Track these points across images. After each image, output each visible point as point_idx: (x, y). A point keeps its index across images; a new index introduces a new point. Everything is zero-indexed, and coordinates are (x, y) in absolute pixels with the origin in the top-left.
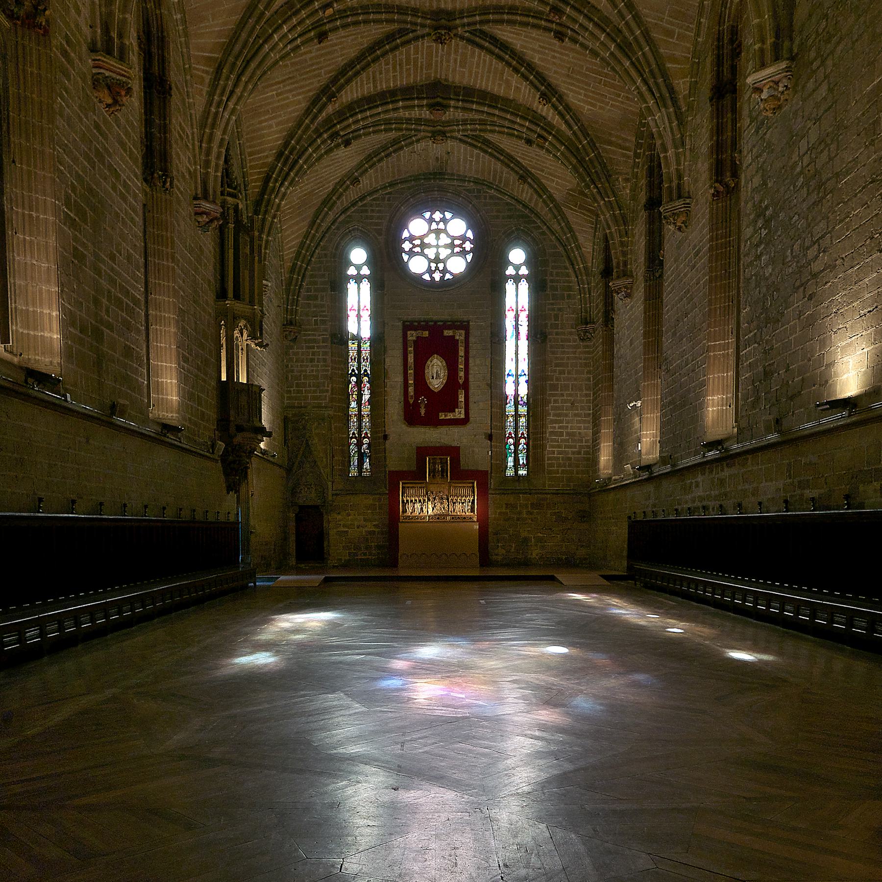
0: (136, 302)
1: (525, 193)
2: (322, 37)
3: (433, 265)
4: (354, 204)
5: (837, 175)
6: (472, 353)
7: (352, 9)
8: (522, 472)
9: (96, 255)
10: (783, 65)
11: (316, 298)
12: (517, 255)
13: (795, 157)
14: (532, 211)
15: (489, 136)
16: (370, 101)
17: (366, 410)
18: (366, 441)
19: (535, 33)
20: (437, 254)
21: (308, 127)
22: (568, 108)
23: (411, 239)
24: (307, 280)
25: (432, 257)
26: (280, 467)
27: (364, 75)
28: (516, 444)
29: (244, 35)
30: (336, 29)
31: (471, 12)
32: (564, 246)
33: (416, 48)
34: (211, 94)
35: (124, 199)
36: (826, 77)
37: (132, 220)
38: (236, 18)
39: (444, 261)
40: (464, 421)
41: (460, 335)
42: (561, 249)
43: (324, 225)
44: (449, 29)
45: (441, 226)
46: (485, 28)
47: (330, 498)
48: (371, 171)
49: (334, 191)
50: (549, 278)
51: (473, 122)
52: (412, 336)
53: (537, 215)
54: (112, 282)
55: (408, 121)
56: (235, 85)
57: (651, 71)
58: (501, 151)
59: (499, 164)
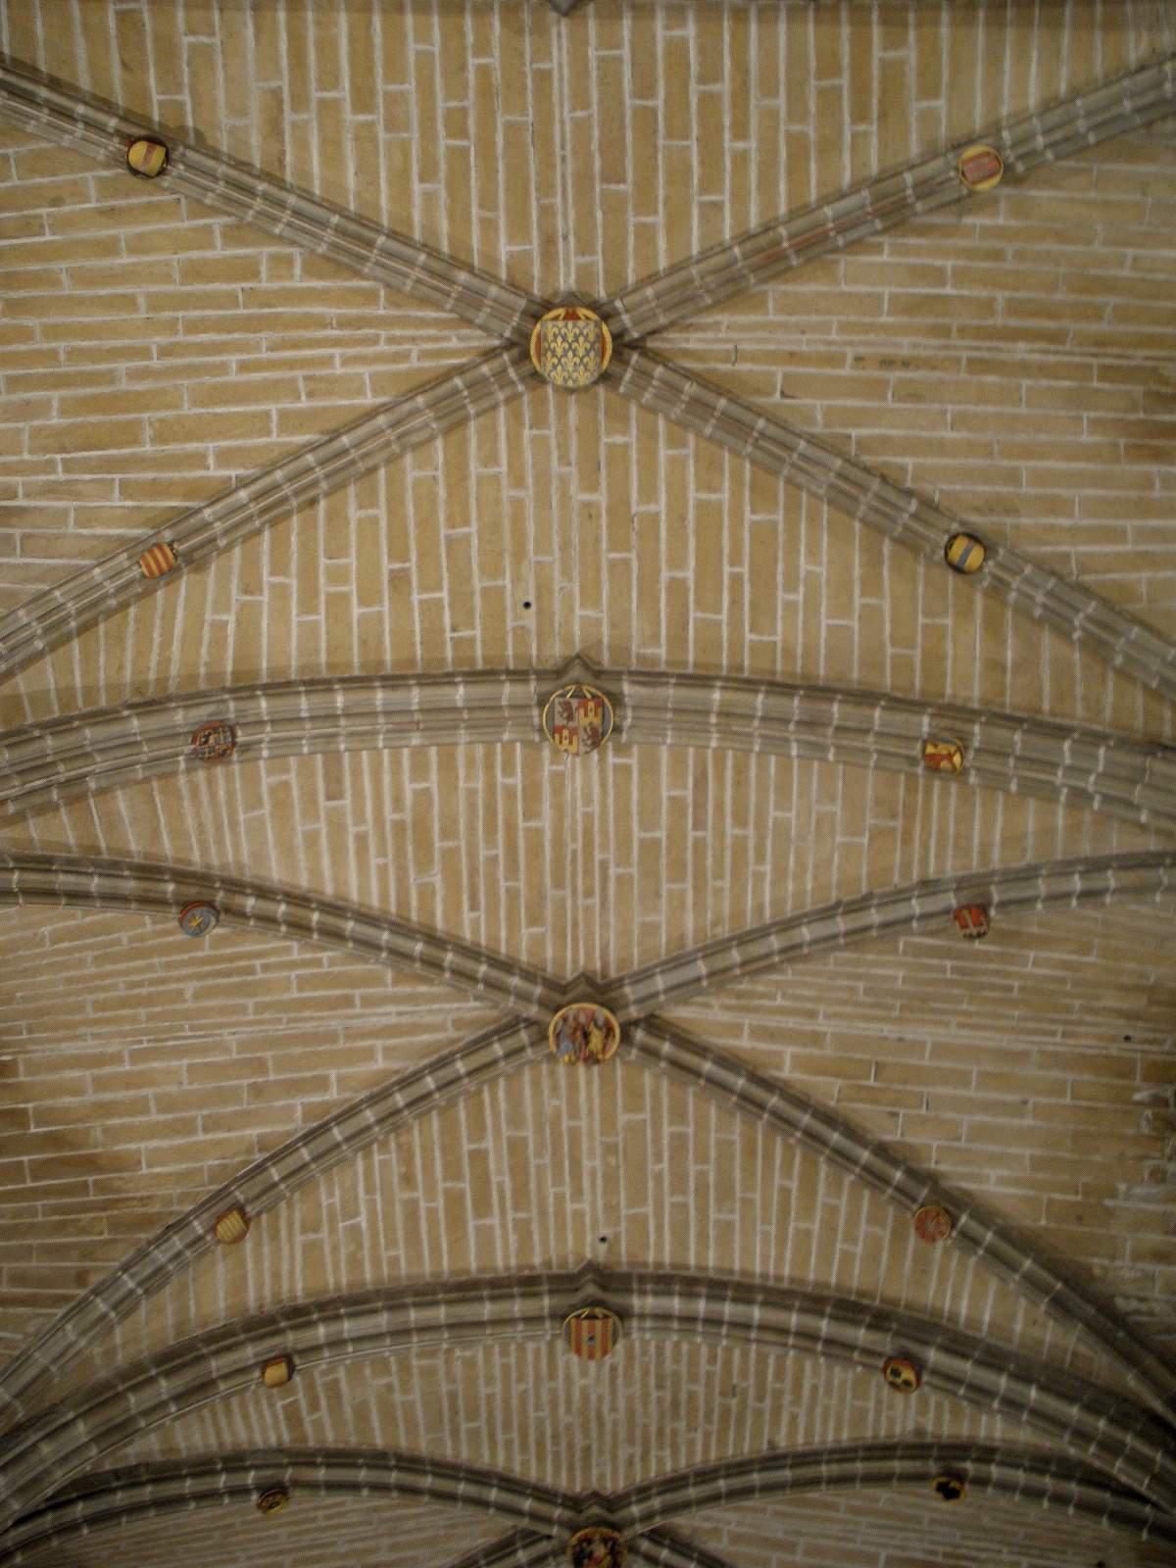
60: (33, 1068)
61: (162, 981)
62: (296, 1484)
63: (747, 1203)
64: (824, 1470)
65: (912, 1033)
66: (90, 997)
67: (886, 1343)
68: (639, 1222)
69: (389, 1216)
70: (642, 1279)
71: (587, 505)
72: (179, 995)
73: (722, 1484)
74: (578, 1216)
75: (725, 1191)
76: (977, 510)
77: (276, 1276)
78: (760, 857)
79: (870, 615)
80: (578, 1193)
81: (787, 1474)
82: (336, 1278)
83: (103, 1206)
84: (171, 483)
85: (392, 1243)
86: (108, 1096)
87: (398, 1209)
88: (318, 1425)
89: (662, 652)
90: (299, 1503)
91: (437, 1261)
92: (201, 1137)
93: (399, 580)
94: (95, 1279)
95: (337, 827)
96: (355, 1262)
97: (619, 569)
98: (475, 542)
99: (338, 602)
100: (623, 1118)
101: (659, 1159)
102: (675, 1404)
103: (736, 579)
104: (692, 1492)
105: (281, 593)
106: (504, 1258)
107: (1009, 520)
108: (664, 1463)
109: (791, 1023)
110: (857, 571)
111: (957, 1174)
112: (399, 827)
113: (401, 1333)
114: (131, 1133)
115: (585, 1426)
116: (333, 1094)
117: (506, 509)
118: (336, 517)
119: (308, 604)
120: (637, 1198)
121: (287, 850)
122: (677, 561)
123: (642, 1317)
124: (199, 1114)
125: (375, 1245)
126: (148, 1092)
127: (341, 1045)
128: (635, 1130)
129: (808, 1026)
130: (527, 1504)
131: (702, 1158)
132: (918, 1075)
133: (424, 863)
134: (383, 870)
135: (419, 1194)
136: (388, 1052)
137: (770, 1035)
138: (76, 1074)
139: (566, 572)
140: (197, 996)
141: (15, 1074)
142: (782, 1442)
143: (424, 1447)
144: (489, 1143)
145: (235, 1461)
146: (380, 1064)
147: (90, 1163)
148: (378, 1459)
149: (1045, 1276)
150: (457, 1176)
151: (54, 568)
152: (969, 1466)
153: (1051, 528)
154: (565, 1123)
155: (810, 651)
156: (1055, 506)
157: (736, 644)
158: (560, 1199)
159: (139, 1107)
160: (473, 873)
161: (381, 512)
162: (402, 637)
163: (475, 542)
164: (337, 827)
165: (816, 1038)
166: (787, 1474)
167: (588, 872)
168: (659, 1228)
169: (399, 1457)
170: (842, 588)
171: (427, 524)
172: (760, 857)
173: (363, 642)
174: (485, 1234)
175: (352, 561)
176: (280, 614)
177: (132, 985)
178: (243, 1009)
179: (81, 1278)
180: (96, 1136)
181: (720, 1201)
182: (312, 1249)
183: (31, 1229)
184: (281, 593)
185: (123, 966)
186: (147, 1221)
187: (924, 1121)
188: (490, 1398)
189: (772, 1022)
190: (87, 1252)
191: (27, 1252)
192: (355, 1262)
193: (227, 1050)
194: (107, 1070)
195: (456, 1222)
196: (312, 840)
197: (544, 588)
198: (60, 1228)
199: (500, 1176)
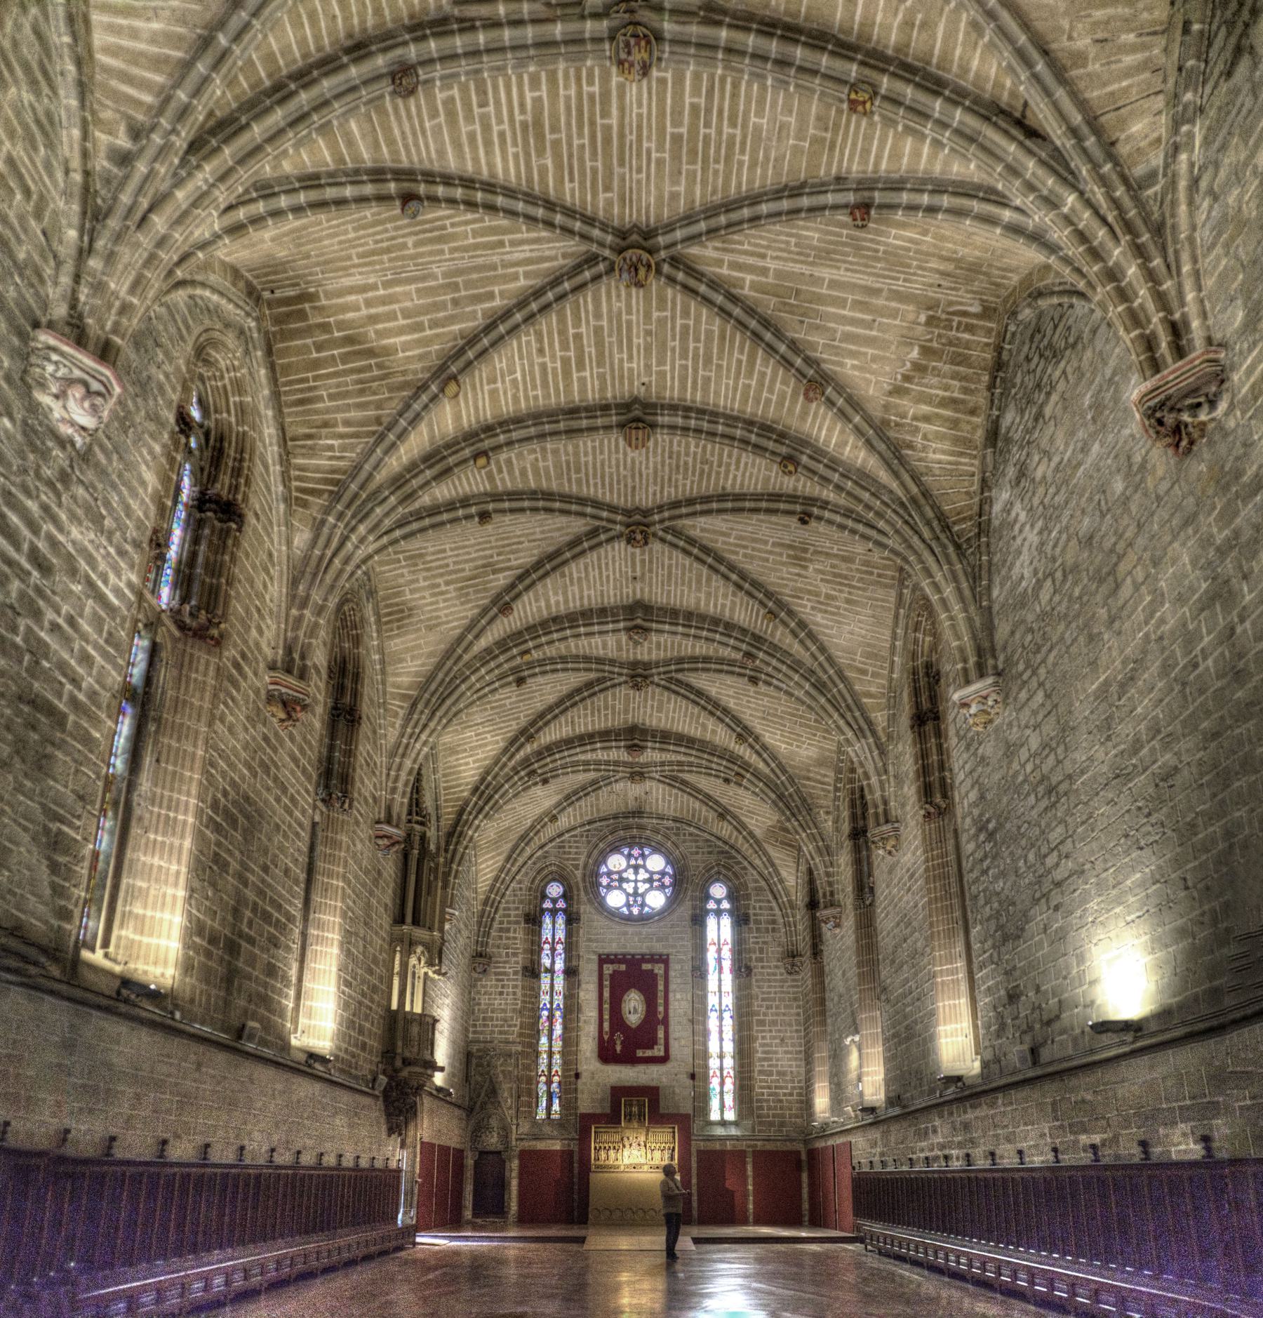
1: (725, 830)
2: (520, 681)
4: (551, 841)
6: (672, 987)
7: (551, 658)
11: (508, 930)
14: (732, 847)
15: (686, 777)
16: (568, 743)
19: (729, 680)
21: (505, 765)
22: (765, 747)
23: (609, 874)
24: (501, 912)
27: (563, 719)
29: (440, 676)
30: (534, 675)
31: (667, 663)
33: (614, 695)
38: (434, 660)
40: (664, 1059)
41: (659, 969)
42: (763, 883)
43: (521, 861)
44: (646, 677)
45: (640, 862)
46: (680, 676)
48: (570, 809)
49: (532, 827)
50: (751, 912)
51: (671, 763)
52: (608, 969)
53: (738, 851)
55: (607, 763)
56: (430, 719)
57: (848, 706)
58: (699, 791)
59: (697, 805)
60: (329, 295)
61: (393, 238)
63: (719, 367)
64: (747, 504)
66: (353, 251)
68: (662, 374)
69: (532, 372)
70: (663, 407)
72: (404, 246)
73: (698, 507)
74: (631, 370)
75: (708, 361)
80: (630, 358)
81: (729, 505)
85: (534, 387)
86: (373, 311)
88: (503, 480)
90: (496, 518)
92: (428, 332)
100: (655, 314)
102: (678, 467)
106: (592, 396)
108: (670, 494)
109: (751, 260)
115: (633, 477)
116: (497, 302)
120: (661, 362)
123: (663, 427)
124: (425, 319)
125: (526, 390)
126: (396, 306)
127: (500, 271)
128: (661, 322)
129: (761, 263)
130: (605, 514)
131: (697, 340)
132: (820, 299)
135: (547, 359)
138: (352, 298)
140: (416, 245)
141: (319, 299)
142: (729, 489)
143: (554, 486)
144: (583, 329)
146: (522, 282)
154: (624, 317)
158: (621, 360)
159: (391, 316)
165: (764, 271)
166: (729, 505)
168: (673, 378)
169: (543, 493)
174: (582, 381)
177: (376, 242)
178: (442, 252)
181: (705, 366)
182: (494, 393)
185: (371, 231)
188: (586, 463)
189: (742, 259)
192: (516, 399)
193: (436, 278)
194: (370, 294)
195: (567, 374)
199: (590, 350)
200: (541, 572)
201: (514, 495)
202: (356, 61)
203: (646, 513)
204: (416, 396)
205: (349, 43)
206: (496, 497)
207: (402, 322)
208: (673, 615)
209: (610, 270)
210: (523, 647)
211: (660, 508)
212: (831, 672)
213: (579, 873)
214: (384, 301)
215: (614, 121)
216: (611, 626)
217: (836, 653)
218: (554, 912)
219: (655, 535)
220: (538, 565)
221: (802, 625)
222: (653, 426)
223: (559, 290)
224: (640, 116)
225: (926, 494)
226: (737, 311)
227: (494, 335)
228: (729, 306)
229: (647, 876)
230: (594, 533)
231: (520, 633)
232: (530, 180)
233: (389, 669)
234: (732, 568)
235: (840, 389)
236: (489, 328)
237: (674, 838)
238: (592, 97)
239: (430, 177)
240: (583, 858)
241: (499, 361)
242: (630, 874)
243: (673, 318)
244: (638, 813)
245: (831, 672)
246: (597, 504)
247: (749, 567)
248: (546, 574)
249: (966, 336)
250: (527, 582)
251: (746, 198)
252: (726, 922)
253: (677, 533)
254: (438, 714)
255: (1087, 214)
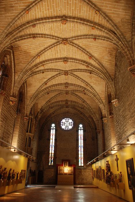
0: (11, 133)
1: (82, 116)
2: (48, 94)
3: (66, 127)
5: (126, 116)
8: (82, 165)
9: (5, 126)
10: (117, 99)
12: (81, 126)
13: (120, 113)
14: (83, 118)
17: (53, 152)
18: (53, 158)
20: (67, 125)
22: (87, 104)
23: (63, 123)
25: (66, 126)
26: (36, 163)
28: (81, 159)
32: (89, 124)
34: (30, 101)
35: (12, 117)
36: (122, 101)
37: (13, 120)
39: (68, 126)
42: (88, 125)
45: (68, 121)
47: (45, 169)
49: (50, 115)
53: (84, 119)
54: (7, 130)
56: (34, 100)
59: (77, 112)
62: (45, 72)
63: (77, 54)
65: (90, 44)
67: (87, 65)
68: (69, 54)
70: (69, 58)
71: (65, 2)
75: (76, 53)
76: (99, 6)
77: (42, 59)
78: (79, 31)
79: (89, 14)
80: (65, 52)
81: (80, 71)
82: (47, 59)
83: (29, 56)
84: (27, 2)
87: (51, 54)
89: (71, 15)
91: (54, 57)
93: (48, 9)
94: (29, 61)
95: (45, 28)
96: (48, 57)
97: (68, 8)
98: (55, 5)
99: (43, 11)
101: (71, 50)
103: (78, 9)
104: (73, 71)
105: (38, 11)
106: (59, 57)
107: (102, 7)
108: (71, 69)
109: (81, 42)
110: (88, 10)
111: (93, 54)
112: (50, 28)
113: (52, 62)
114: (30, 50)
117: (58, 2)
118: (42, 4)
119: (41, 12)
120: (69, 53)
121: (41, 30)
122: (73, 7)
124: (35, 49)
126: (31, 47)
130: (61, 71)
132: (91, 47)
133: (52, 31)
134: (49, 31)
136: (50, 43)
137: (79, 43)
139: (63, 8)
142: (80, 68)
145: (40, 71)
146: (49, 44)
147: (28, 53)
148: (50, 69)
149: (98, 62)
150: (55, 51)
151: (18, 12)
152: (92, 72)
153: (105, 9)
155: (84, 16)
156: (106, 7)
157: (78, 15)
158: (63, 53)
160: (56, 31)
161: (46, 3)
162: (49, 14)
163: (55, 5)
164: (45, 28)
165: (83, 43)
166: (80, 71)
167: (65, 31)
170: (87, 11)
171: (50, 4)
172: (79, 31)
173: (46, 14)
175: (44, 8)
176: (38, 13)
179: (28, 61)
180: (28, 51)
183: (24, 58)
184: (38, 11)
186: (32, 57)
187: (91, 50)
189: (80, 42)
190: (28, 59)
191: (24, 60)
192: (48, 57)
195: (55, 54)
196: (43, 30)
197: (61, 9)
198: (26, 58)
199: (59, 51)
200: (51, 79)
201: (48, 69)
202: (28, 24)
203: (67, 71)
204: (34, 58)
205: (27, 22)
206: (45, 70)
207: (32, 49)
208: (72, 84)
209: (61, 43)
210: (48, 89)
211: (70, 70)
212: (96, 94)
213: (57, 123)
214: (30, 47)
215: (62, 28)
216: (62, 86)
217: (97, 91)
218: (53, 129)
219: (69, 74)
220: (51, 78)
221: (92, 87)
222: (68, 61)
223: (54, 45)
224: (65, 27)
225: (107, 72)
226: (79, 48)
227: (45, 50)
228: (78, 47)
229: (69, 123)
230: (60, 73)
231: (48, 87)
232: (50, 33)
233: (28, 93)
234: (81, 78)
235: (94, 57)
236: (44, 49)
237: (73, 117)
238: (59, 25)
239: (37, 34)
240: (58, 120)
241: (46, 53)
242: (66, 123)
243: (71, 48)
244: (68, 112)
245: (96, 94)
246: (60, 70)
247: (83, 78)
248: (52, 79)
249: (112, 52)
250: (49, 80)
251: (80, 36)
252: (82, 131)
253: (72, 74)
254: (35, 99)
255: (122, 45)
